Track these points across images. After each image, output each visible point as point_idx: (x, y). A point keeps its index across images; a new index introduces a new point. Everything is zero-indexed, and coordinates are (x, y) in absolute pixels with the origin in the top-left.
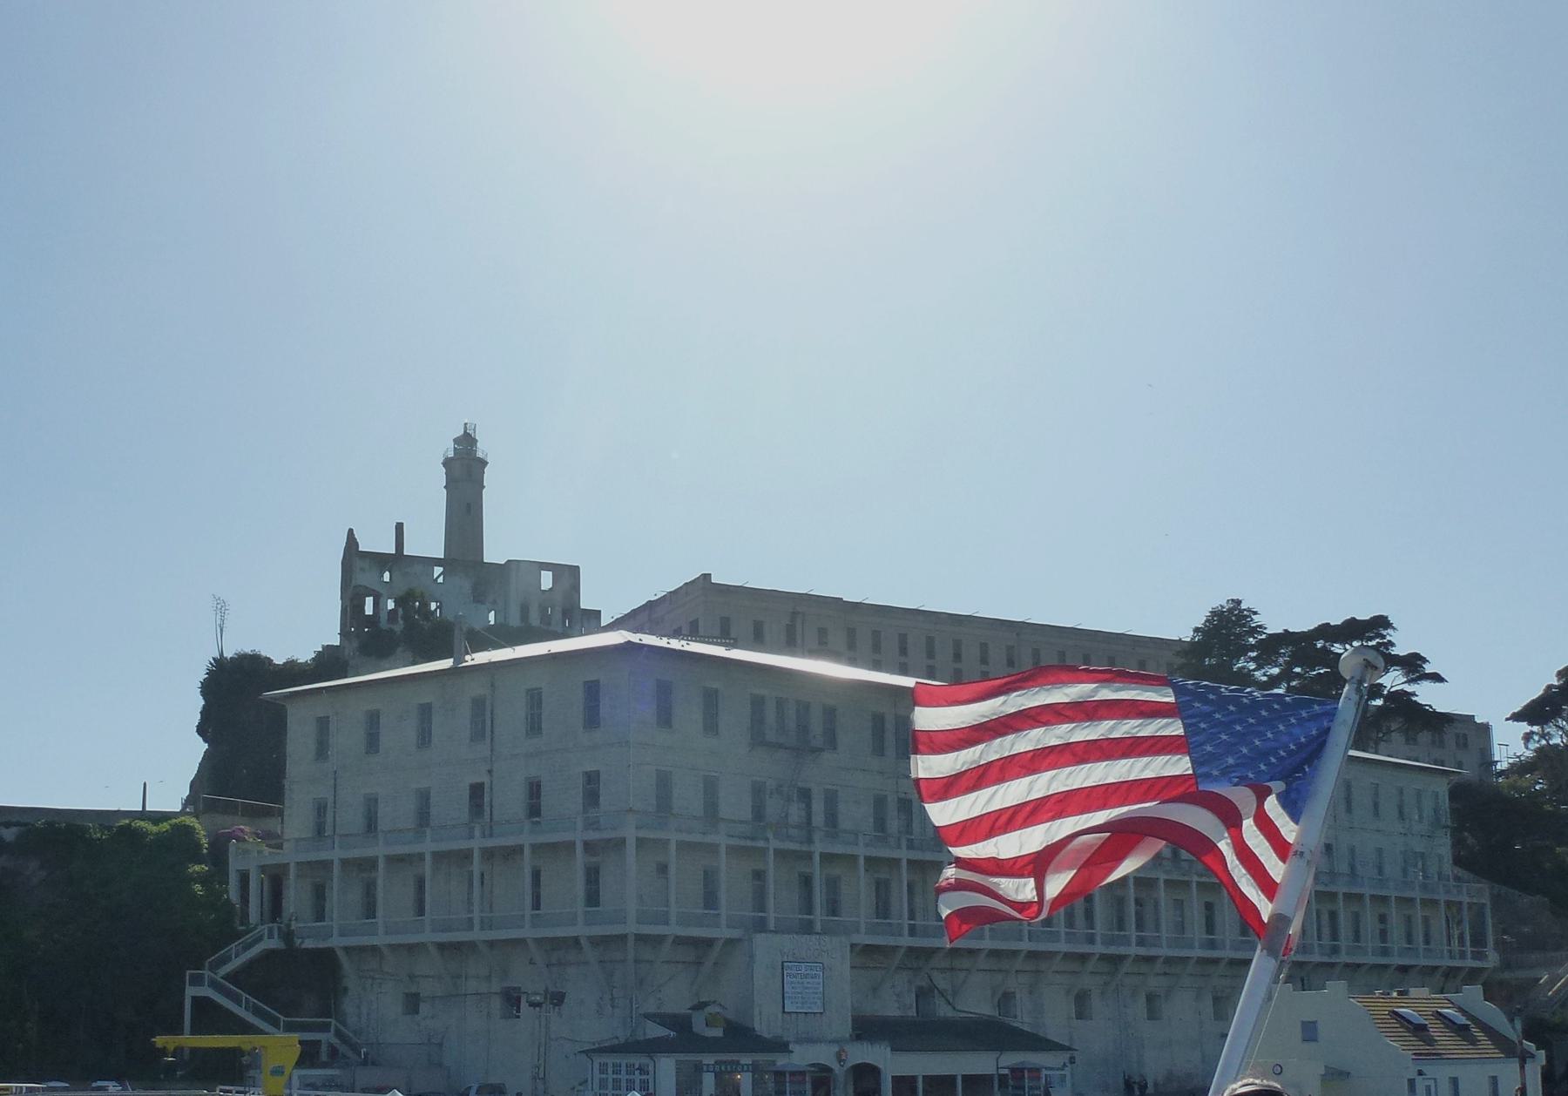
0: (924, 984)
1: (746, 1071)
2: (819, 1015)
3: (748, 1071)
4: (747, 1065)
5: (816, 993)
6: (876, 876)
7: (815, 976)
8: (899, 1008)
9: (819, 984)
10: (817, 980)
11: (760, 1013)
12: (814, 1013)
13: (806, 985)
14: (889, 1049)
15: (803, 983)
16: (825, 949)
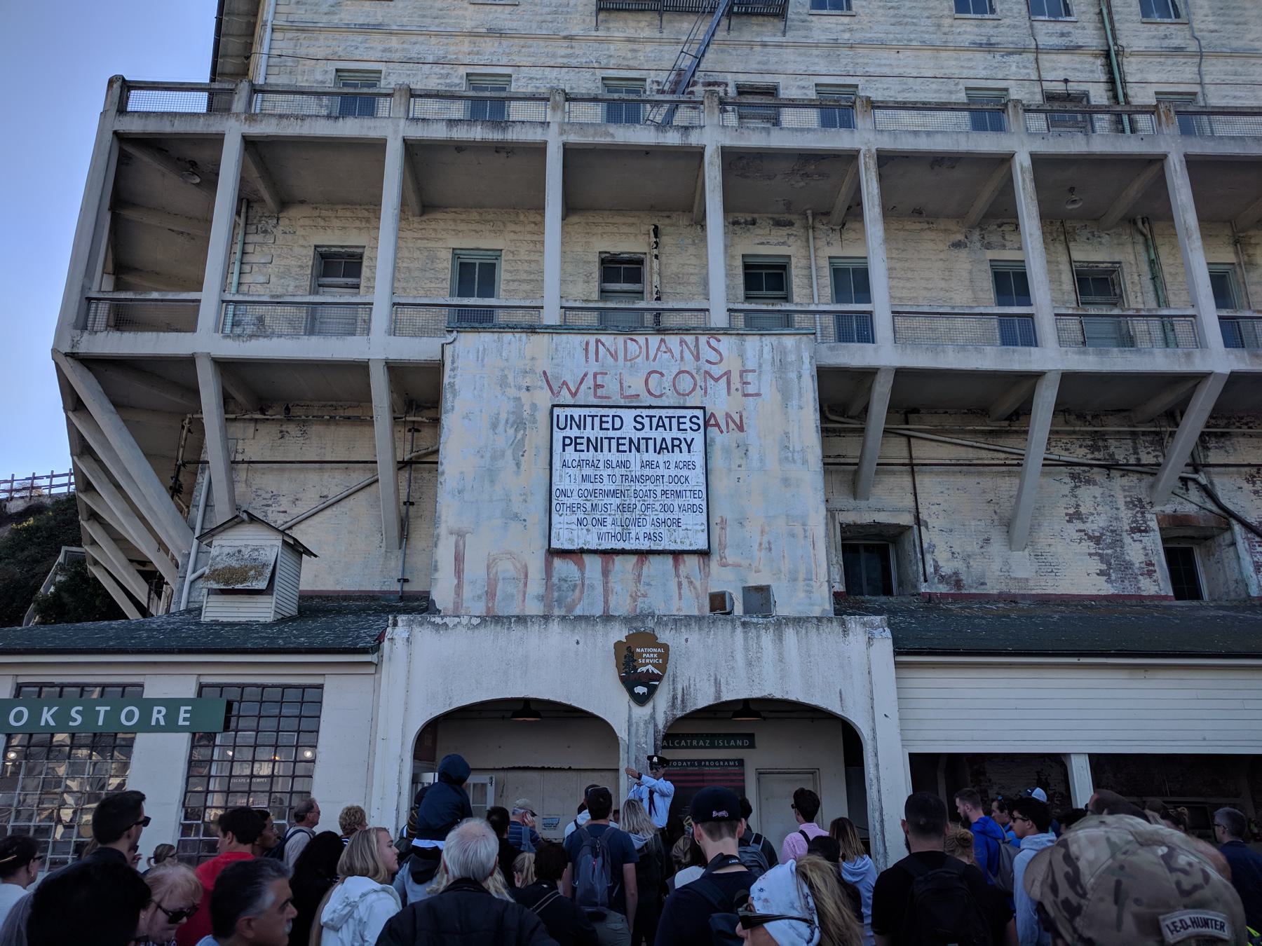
0: (1189, 509)
1: (158, 729)
2: (692, 562)
3: (171, 726)
4: (173, 705)
5: (678, 494)
6: (991, 255)
7: (676, 445)
8: (1101, 573)
9: (688, 465)
10: (676, 456)
11: (459, 559)
12: (677, 554)
13: (636, 469)
14: (884, 645)
15: (624, 464)
16: (717, 371)
